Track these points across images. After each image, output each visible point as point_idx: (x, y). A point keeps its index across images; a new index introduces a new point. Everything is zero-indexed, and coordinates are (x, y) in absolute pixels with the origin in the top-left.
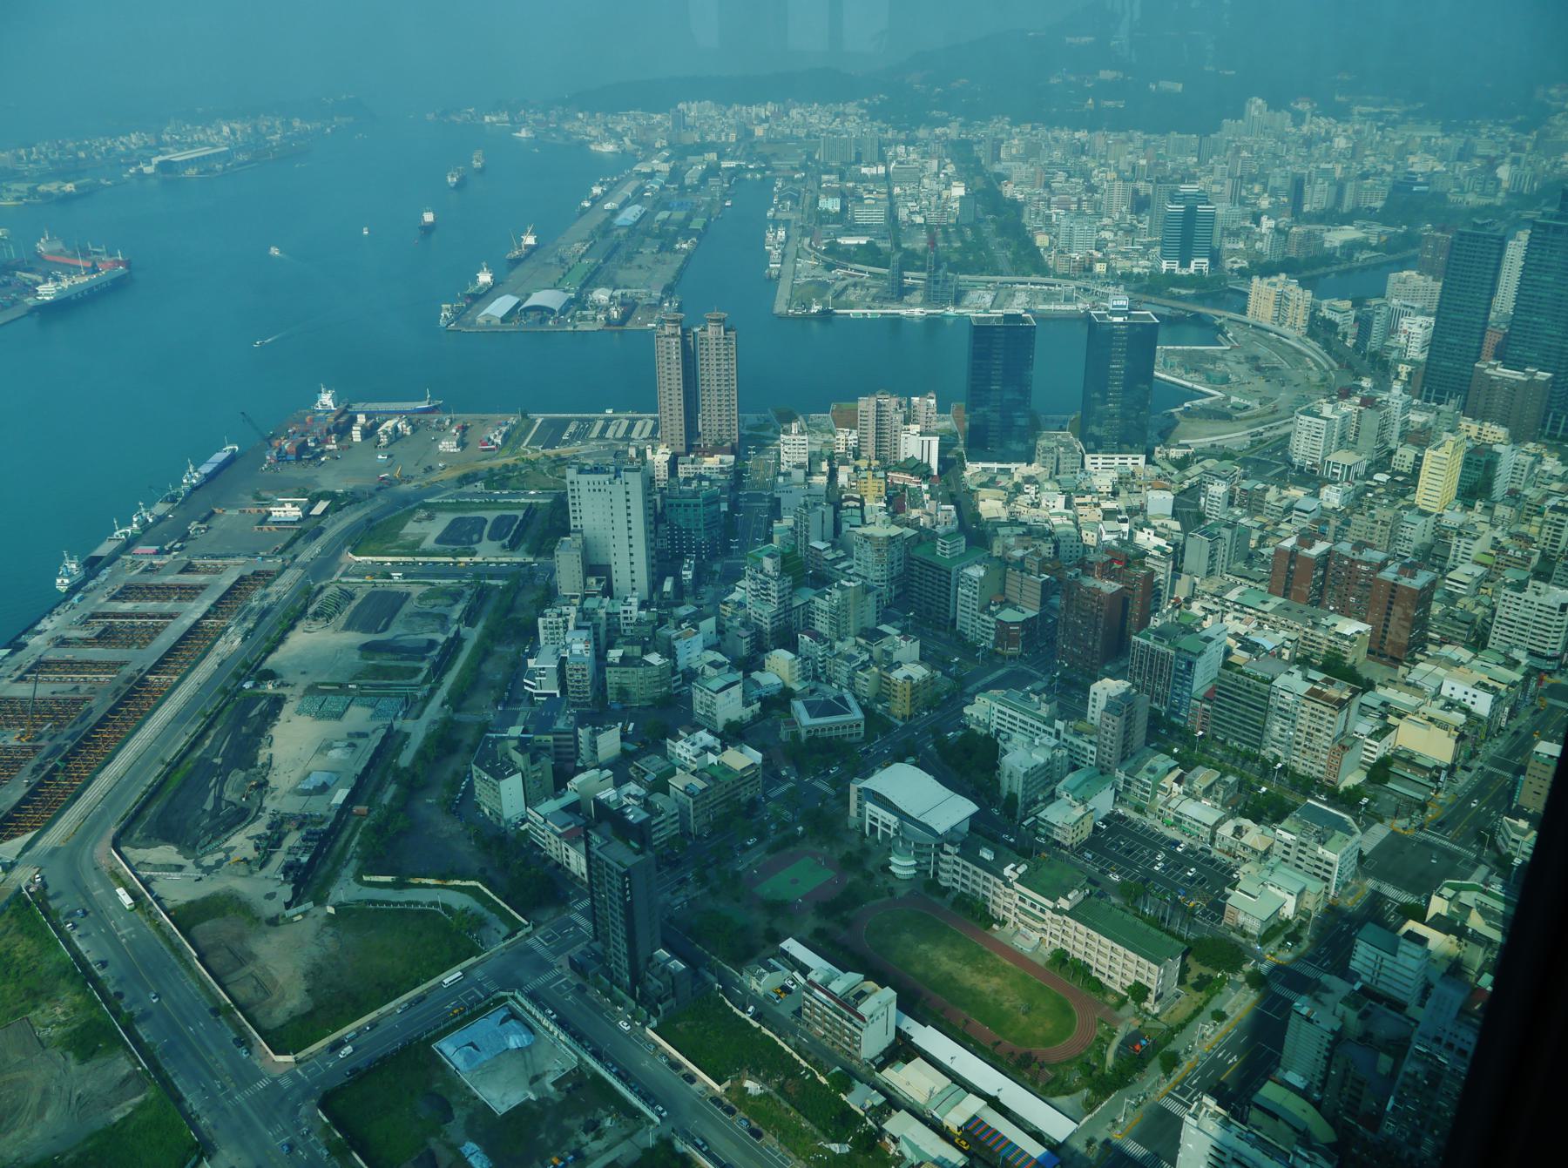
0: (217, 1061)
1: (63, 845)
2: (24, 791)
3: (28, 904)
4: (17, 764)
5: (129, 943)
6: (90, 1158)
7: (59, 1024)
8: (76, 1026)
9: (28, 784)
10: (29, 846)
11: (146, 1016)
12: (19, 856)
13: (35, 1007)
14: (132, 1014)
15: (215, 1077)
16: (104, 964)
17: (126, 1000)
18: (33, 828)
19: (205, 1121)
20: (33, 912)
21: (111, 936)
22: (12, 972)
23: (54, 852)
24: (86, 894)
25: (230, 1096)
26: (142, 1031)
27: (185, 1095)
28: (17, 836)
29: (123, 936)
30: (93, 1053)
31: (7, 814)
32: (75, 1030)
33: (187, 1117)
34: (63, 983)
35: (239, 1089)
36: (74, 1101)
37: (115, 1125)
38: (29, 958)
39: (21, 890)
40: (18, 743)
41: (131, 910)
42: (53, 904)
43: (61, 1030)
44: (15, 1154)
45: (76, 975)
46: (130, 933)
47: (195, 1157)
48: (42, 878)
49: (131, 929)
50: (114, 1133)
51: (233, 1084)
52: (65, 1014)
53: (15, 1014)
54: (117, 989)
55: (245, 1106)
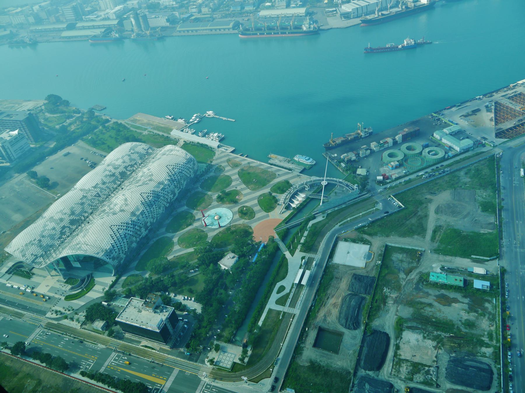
0: (519, 236)
1: (514, 147)
2: (512, 125)
3: (494, 159)
4: (515, 116)
5: (515, 186)
6: (469, 237)
7: (483, 198)
8: (486, 201)
9: (515, 124)
10: (504, 143)
11: (507, 210)
12: (500, 144)
13: (479, 189)
14: (503, 207)
15: (515, 239)
16: (504, 188)
17: (504, 202)
18: (508, 138)
19: (504, 249)
20: (494, 163)
21: (511, 182)
22: (479, 176)
23: (510, 148)
24: (511, 164)
25: (516, 248)
26: (503, 214)
27: (503, 238)
28: (502, 138)
29: (514, 183)
30: (486, 211)
31: (504, 130)
32: (485, 202)
33: (500, 245)
34: (490, 187)
35: (520, 248)
36: (474, 220)
37: (480, 233)
38: (486, 175)
39: (494, 155)
40: (519, 110)
41: (522, 177)
42: (501, 164)
43: (482, 199)
44: (453, 224)
45: (495, 187)
46: (517, 184)
47: (495, 257)
48: (502, 154)
49: (518, 183)
50: (479, 235)
51: (519, 245)
52: (486, 195)
53: (473, 188)
54: (503, 197)
55: (519, 254)
